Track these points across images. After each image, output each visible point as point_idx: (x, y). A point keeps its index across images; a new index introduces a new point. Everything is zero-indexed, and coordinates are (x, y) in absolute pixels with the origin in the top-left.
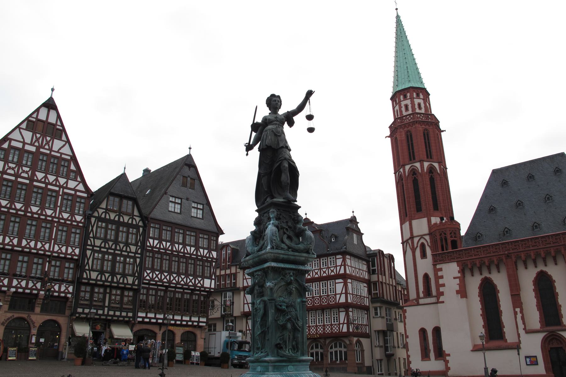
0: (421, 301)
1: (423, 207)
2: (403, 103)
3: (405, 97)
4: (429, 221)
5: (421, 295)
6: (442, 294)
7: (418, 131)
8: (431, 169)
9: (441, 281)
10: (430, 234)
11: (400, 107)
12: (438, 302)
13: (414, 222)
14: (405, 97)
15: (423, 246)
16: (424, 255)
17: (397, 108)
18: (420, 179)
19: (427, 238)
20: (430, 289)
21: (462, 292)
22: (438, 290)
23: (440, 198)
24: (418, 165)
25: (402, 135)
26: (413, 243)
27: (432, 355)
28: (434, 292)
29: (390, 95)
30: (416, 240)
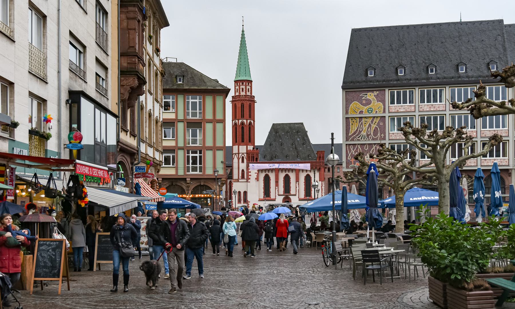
0: (240, 181)
1: (245, 141)
2: (241, 87)
3: (243, 84)
4: (247, 148)
5: (240, 178)
6: (250, 179)
7: (246, 104)
8: (250, 123)
9: (250, 174)
10: (247, 153)
11: (240, 89)
12: (247, 181)
13: (240, 147)
14: (243, 84)
15: (243, 157)
16: (243, 161)
17: (237, 87)
18: (245, 128)
19: (245, 154)
20: (245, 176)
21: (257, 179)
22: (247, 177)
23: (252, 137)
24: (245, 121)
25: (239, 105)
26: (239, 156)
27: (242, 201)
28: (246, 177)
29: (234, 79)
30: (240, 155)
